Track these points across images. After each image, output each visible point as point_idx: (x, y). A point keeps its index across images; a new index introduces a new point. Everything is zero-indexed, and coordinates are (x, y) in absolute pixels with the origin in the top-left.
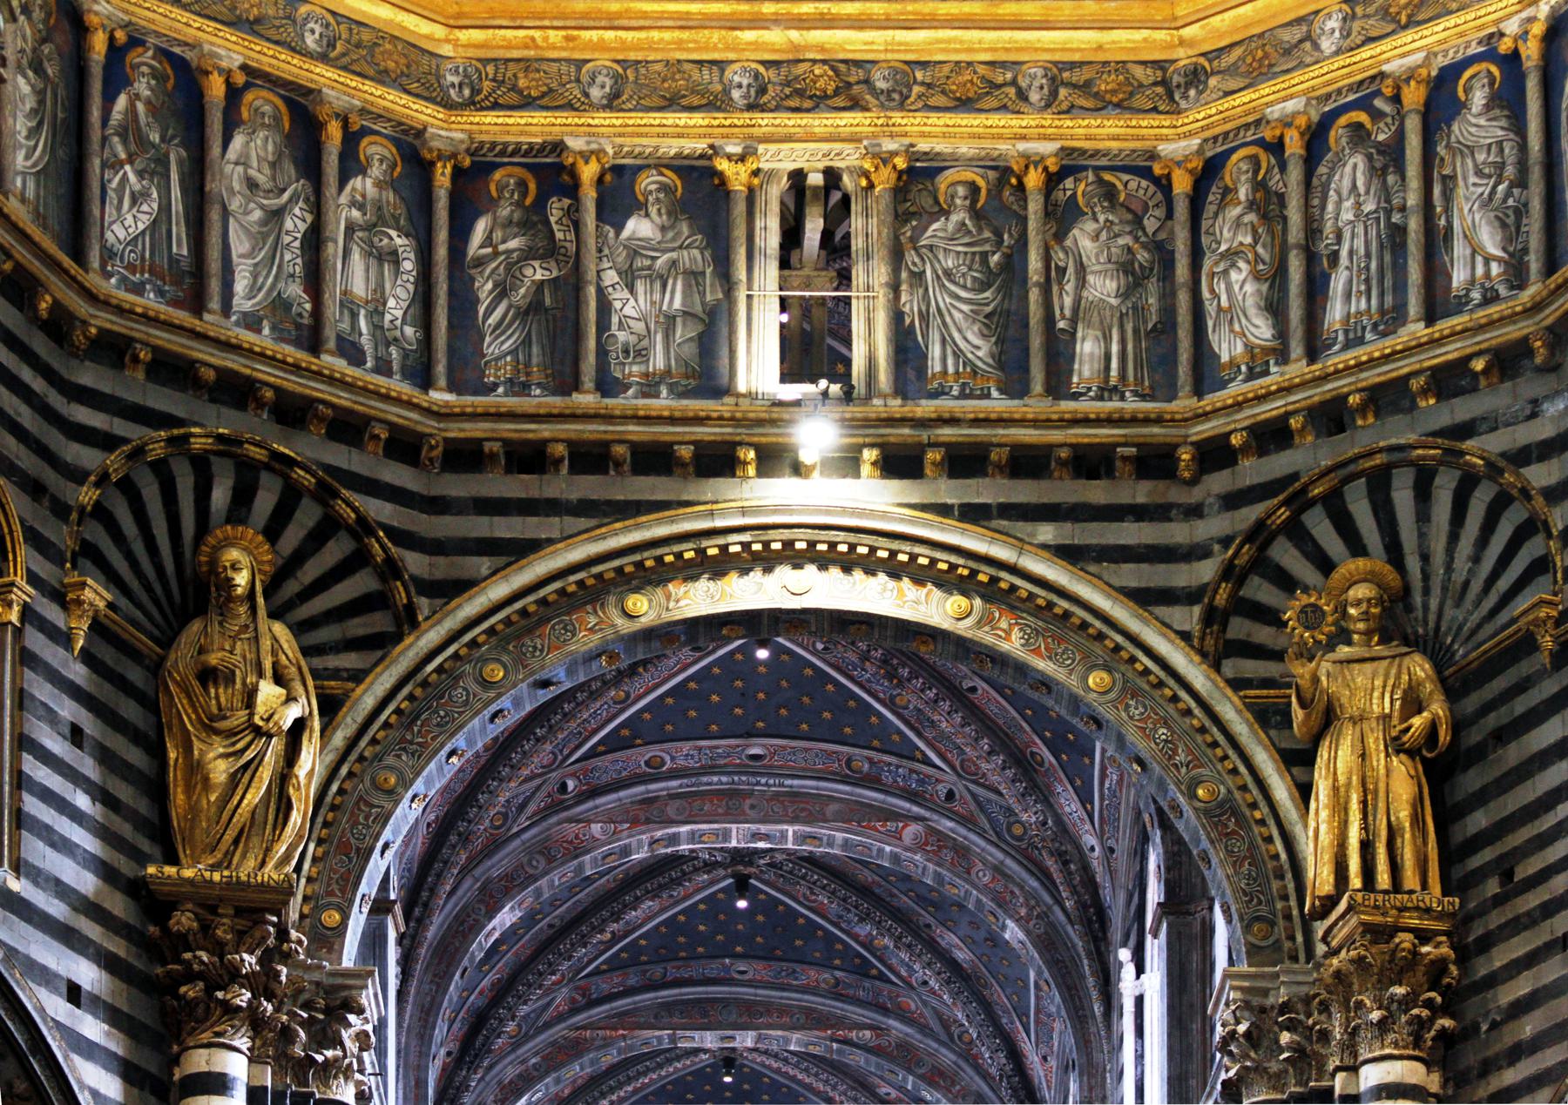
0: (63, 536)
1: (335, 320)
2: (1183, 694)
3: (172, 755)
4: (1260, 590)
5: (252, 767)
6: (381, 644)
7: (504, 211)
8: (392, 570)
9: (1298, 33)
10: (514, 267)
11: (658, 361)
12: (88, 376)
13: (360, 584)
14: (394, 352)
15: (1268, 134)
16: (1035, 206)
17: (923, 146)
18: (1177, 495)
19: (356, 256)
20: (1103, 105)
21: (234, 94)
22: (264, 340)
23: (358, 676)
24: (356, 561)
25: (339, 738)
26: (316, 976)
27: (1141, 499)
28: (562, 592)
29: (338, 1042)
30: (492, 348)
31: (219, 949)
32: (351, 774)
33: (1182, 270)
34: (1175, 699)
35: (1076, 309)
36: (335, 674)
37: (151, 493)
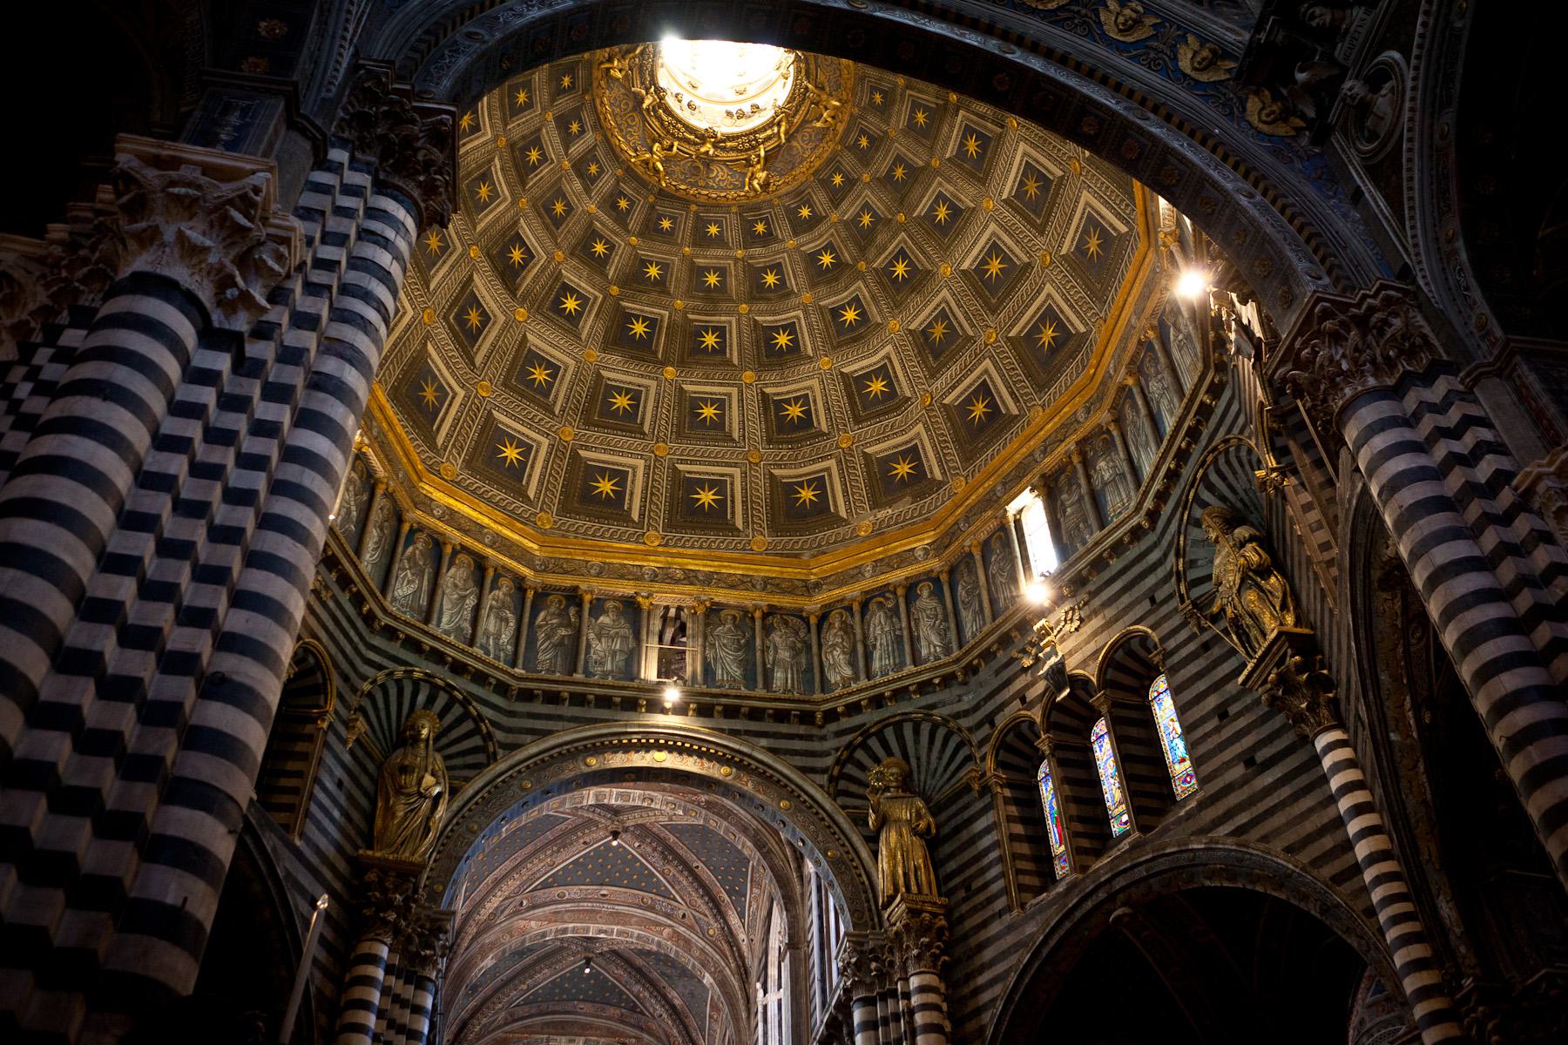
0: (354, 701)
1: (480, 639)
2: (821, 811)
3: (380, 804)
4: (850, 769)
5: (415, 811)
6: (479, 767)
7: (552, 609)
8: (489, 736)
9: (856, 571)
10: (553, 629)
11: (609, 667)
12: (377, 641)
13: (476, 741)
14: (502, 654)
15: (846, 603)
16: (758, 624)
17: (716, 599)
18: (815, 731)
19: (492, 617)
20: (783, 592)
21: (455, 553)
22: (452, 639)
23: (467, 780)
24: (476, 731)
25: (455, 806)
26: (428, 913)
27: (801, 732)
28: (560, 753)
29: (433, 948)
30: (541, 657)
31: (385, 891)
32: (457, 823)
33: (815, 649)
34: (817, 813)
35: (774, 661)
36: (457, 778)
37: (393, 692)
